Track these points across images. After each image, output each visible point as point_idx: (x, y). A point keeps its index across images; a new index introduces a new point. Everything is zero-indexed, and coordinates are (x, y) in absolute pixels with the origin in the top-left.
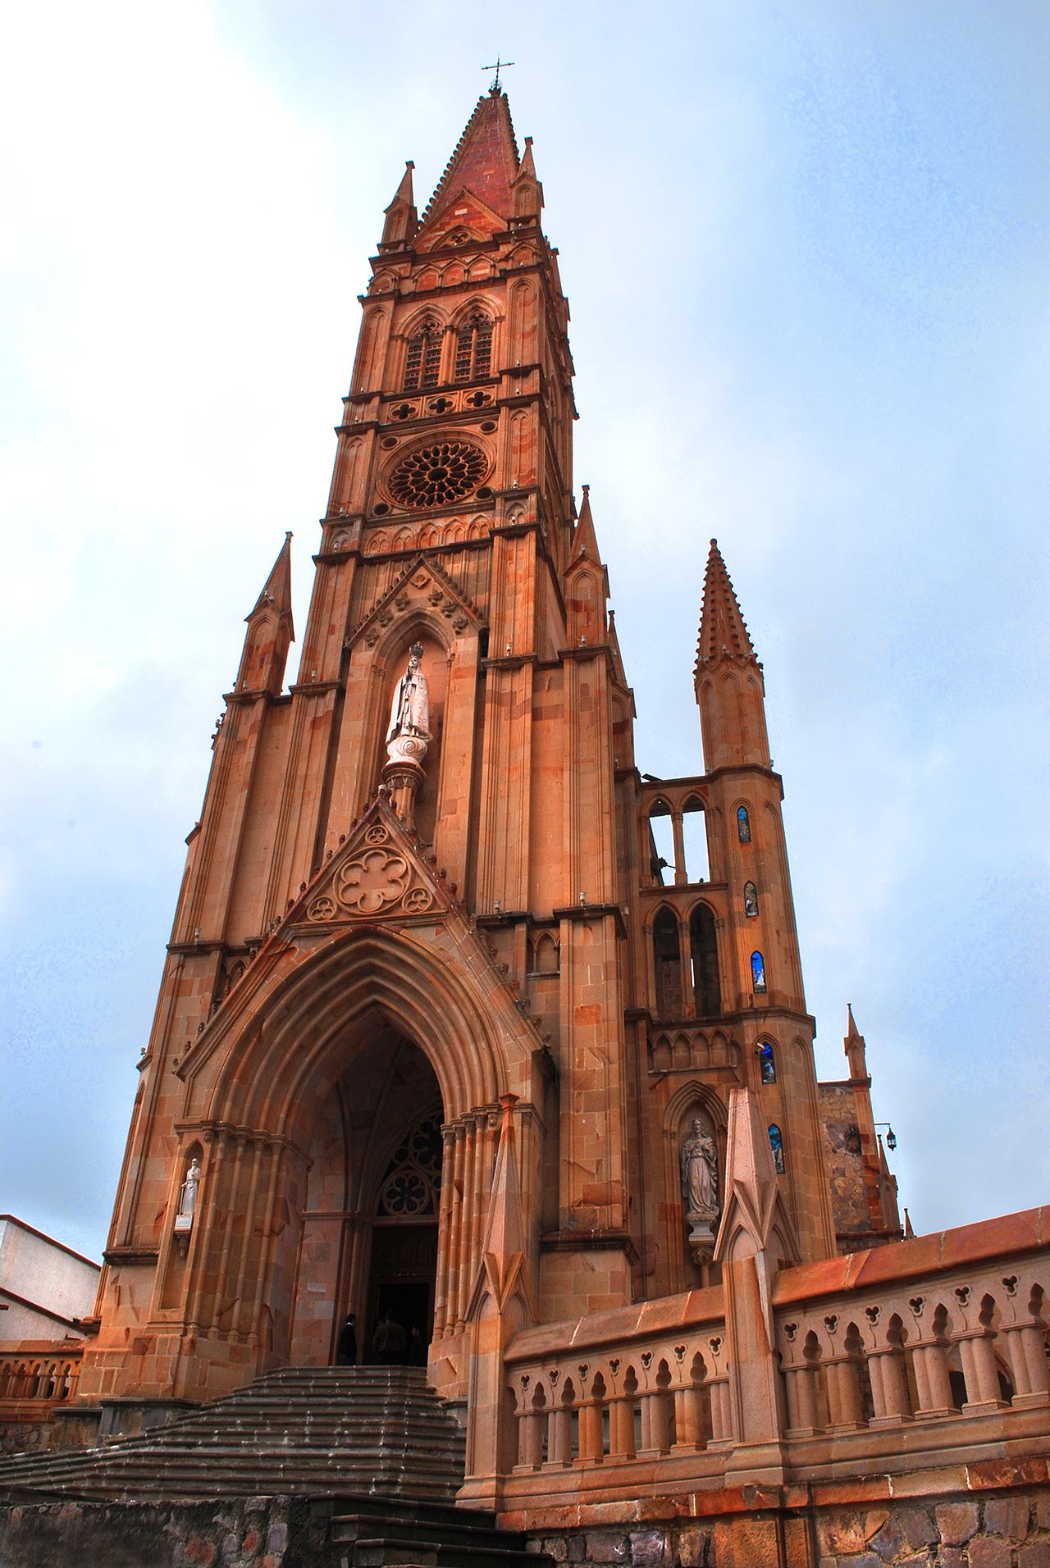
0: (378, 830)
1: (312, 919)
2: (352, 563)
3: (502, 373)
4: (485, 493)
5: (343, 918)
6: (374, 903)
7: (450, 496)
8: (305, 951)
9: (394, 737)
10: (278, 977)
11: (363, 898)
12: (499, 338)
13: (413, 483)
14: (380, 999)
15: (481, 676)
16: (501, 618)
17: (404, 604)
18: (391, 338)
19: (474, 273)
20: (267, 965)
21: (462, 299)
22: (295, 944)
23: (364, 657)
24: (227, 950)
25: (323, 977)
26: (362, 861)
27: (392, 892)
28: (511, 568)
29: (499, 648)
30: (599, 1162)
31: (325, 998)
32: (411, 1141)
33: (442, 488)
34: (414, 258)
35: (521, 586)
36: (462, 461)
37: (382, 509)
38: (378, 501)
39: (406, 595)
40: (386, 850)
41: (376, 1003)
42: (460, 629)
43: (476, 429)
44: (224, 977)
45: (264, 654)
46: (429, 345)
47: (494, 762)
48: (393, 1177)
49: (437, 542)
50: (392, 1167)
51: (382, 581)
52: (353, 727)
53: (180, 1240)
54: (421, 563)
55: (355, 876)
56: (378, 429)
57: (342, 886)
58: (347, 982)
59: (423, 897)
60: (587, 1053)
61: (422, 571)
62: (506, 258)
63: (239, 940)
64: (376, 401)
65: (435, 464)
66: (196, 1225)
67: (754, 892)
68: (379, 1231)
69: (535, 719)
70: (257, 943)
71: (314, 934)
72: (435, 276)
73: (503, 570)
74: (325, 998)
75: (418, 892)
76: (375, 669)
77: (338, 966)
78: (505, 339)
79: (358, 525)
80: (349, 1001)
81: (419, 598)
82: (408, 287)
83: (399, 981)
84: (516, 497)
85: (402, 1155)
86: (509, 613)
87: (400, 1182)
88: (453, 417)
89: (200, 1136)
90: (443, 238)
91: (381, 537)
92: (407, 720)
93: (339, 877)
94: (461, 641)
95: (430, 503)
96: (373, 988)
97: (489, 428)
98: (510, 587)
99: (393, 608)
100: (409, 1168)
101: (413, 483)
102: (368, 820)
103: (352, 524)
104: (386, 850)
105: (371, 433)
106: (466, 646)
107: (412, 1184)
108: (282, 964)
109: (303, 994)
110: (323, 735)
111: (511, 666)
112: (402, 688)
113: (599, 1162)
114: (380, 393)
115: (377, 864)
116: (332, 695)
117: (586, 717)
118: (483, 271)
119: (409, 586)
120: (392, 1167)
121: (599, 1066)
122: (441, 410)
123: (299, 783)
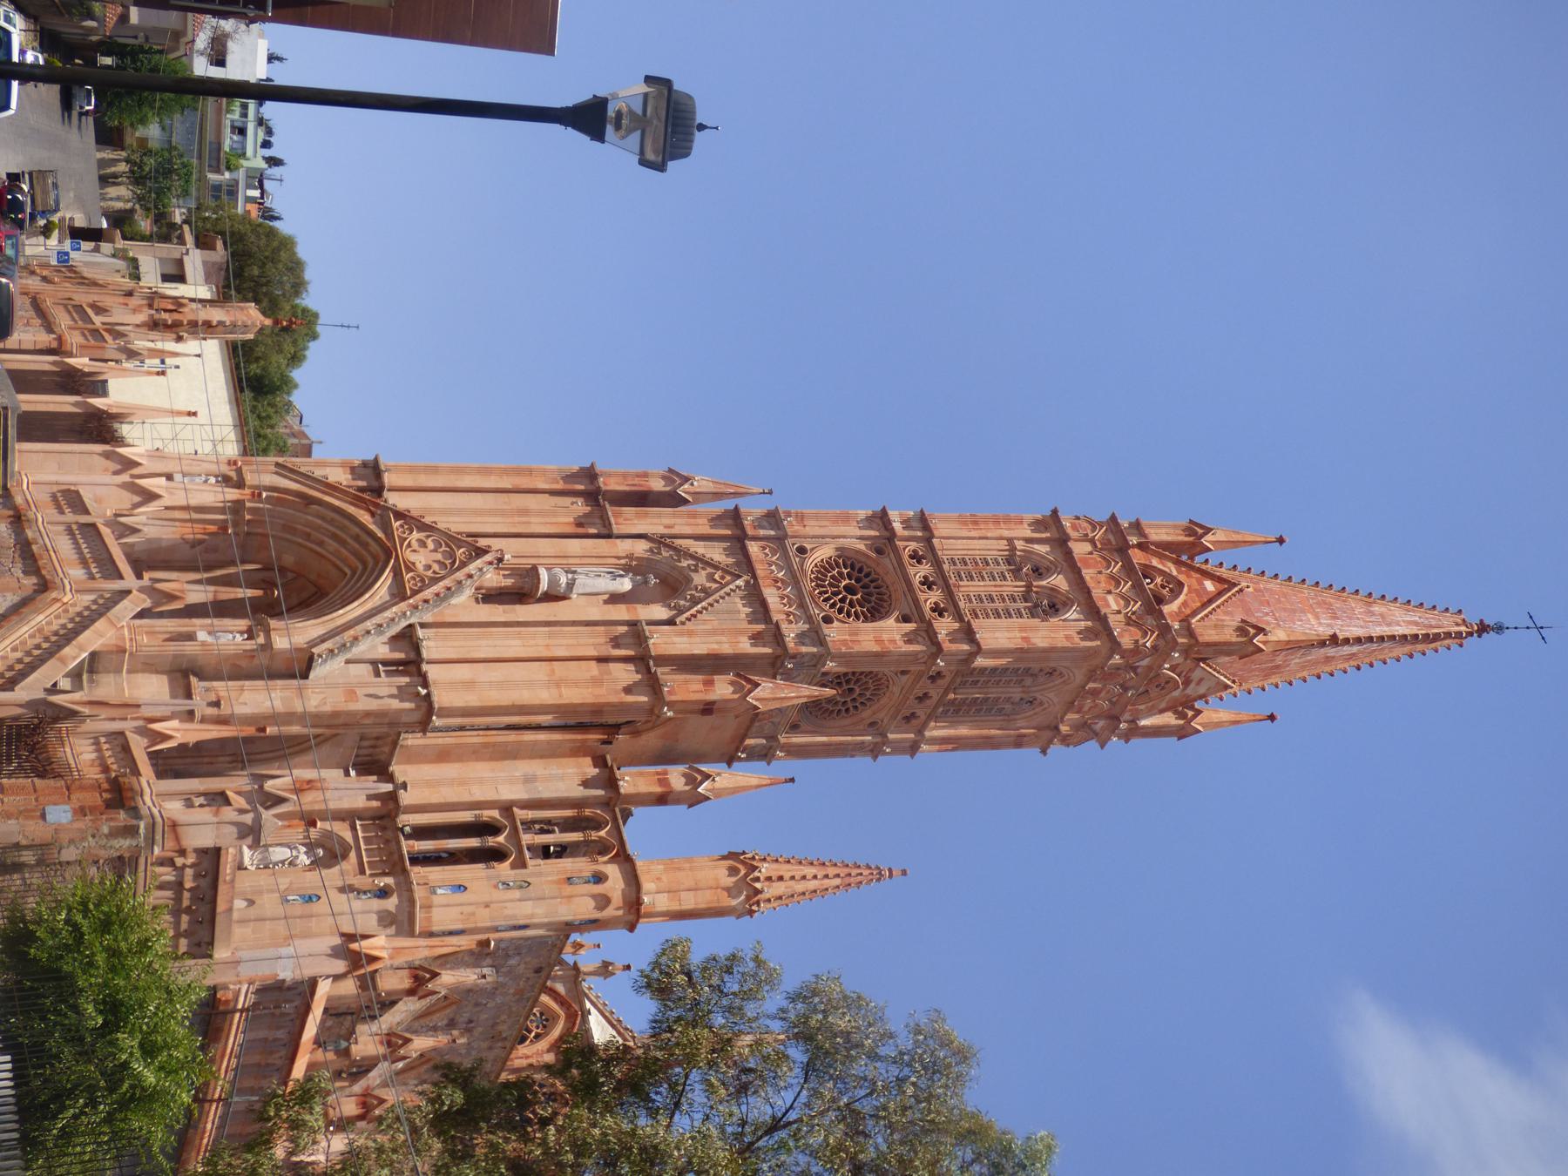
1: (396, 524)
6: (412, 557)
10: (351, 510)
16: (690, 634)
19: (1110, 598)
23: (641, 548)
25: (357, 538)
27: (420, 567)
31: (342, 542)
33: (835, 594)
55: (431, 545)
58: (355, 554)
74: (342, 542)
76: (630, 557)
77: (365, 545)
80: (344, 560)
81: (700, 578)
82: (1080, 549)
84: (814, 635)
114: (932, 536)
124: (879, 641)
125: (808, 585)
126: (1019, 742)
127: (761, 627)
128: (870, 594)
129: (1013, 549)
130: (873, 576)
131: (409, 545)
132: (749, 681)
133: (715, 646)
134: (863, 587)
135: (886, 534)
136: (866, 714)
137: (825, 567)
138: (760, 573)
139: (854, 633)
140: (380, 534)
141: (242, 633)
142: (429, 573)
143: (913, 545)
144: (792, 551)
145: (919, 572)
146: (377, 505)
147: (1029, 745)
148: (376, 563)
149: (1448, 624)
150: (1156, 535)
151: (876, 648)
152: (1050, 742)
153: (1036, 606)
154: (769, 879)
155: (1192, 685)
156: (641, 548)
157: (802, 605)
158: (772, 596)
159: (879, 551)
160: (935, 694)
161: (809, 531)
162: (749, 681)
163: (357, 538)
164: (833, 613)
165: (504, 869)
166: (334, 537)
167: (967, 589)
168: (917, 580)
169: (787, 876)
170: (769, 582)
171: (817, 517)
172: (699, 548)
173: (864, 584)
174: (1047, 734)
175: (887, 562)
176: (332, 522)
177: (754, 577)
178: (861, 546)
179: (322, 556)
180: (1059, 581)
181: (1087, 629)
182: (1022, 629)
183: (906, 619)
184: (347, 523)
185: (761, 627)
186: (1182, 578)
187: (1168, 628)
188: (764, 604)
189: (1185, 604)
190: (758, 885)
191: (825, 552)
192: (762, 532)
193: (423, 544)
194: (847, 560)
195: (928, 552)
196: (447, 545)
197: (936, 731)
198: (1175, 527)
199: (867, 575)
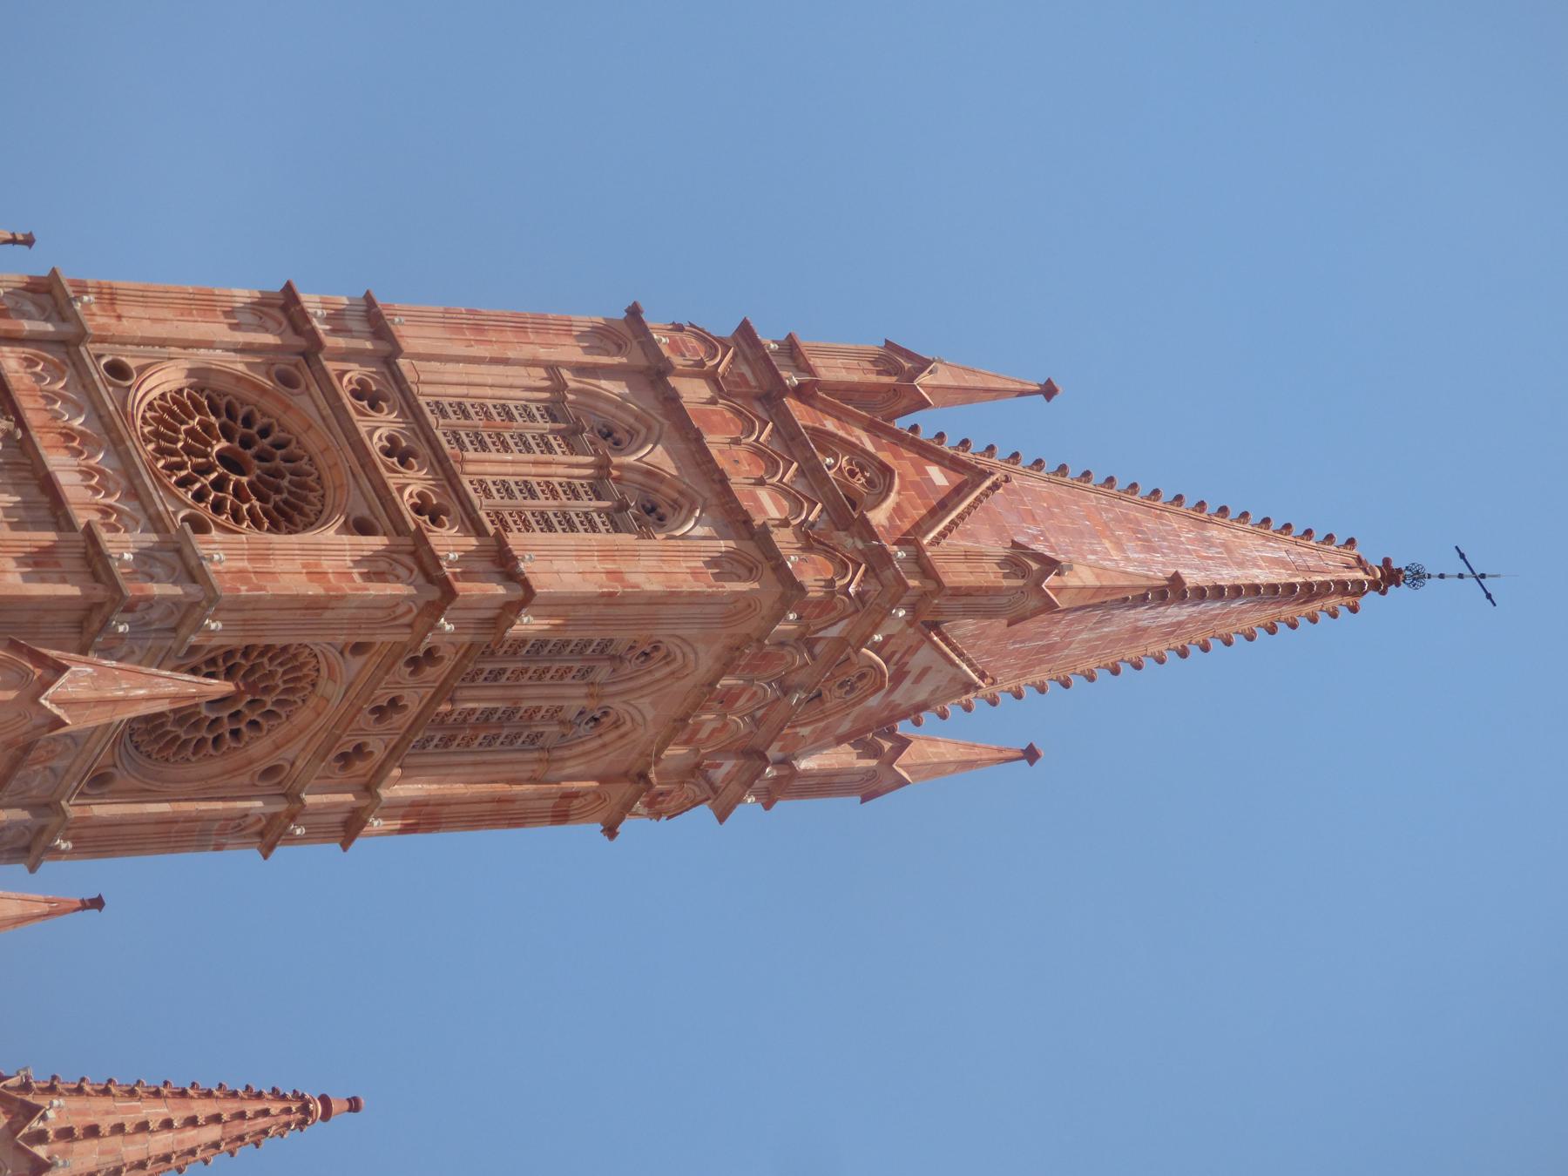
7: (183, 483)
19: (763, 495)
33: (203, 470)
82: (693, 392)
114: (397, 351)
124: (316, 575)
126: (561, 815)
127: (48, 537)
128: (278, 474)
129: (559, 387)
130: (277, 434)
132: (40, 660)
134: (260, 457)
135: (300, 342)
136: (259, 748)
137: (170, 411)
138: (33, 418)
139: (262, 556)
143: (355, 371)
144: (98, 374)
145: (377, 428)
147: (584, 816)
149: (1332, 566)
150: (831, 370)
151: (314, 590)
152: (626, 809)
153: (622, 507)
154: (66, 1134)
155: (907, 683)
157: (134, 492)
158: (63, 468)
159: (287, 380)
160: (413, 701)
161: (128, 327)
162: (40, 660)
164: (204, 510)
167: (483, 467)
168: (375, 444)
169: (105, 1125)
170: (51, 438)
171: (144, 298)
173: (251, 452)
174: (625, 789)
175: (307, 403)
177: (20, 423)
178: (238, 365)
180: (657, 456)
181: (729, 556)
182: (607, 554)
183: (362, 527)
185: (48, 537)
186: (885, 457)
187: (887, 558)
188: (48, 485)
189: (898, 510)
190: (41, 1151)
191: (167, 379)
192: (27, 326)
195: (389, 385)
197: (401, 790)
198: (859, 355)
199: (264, 432)
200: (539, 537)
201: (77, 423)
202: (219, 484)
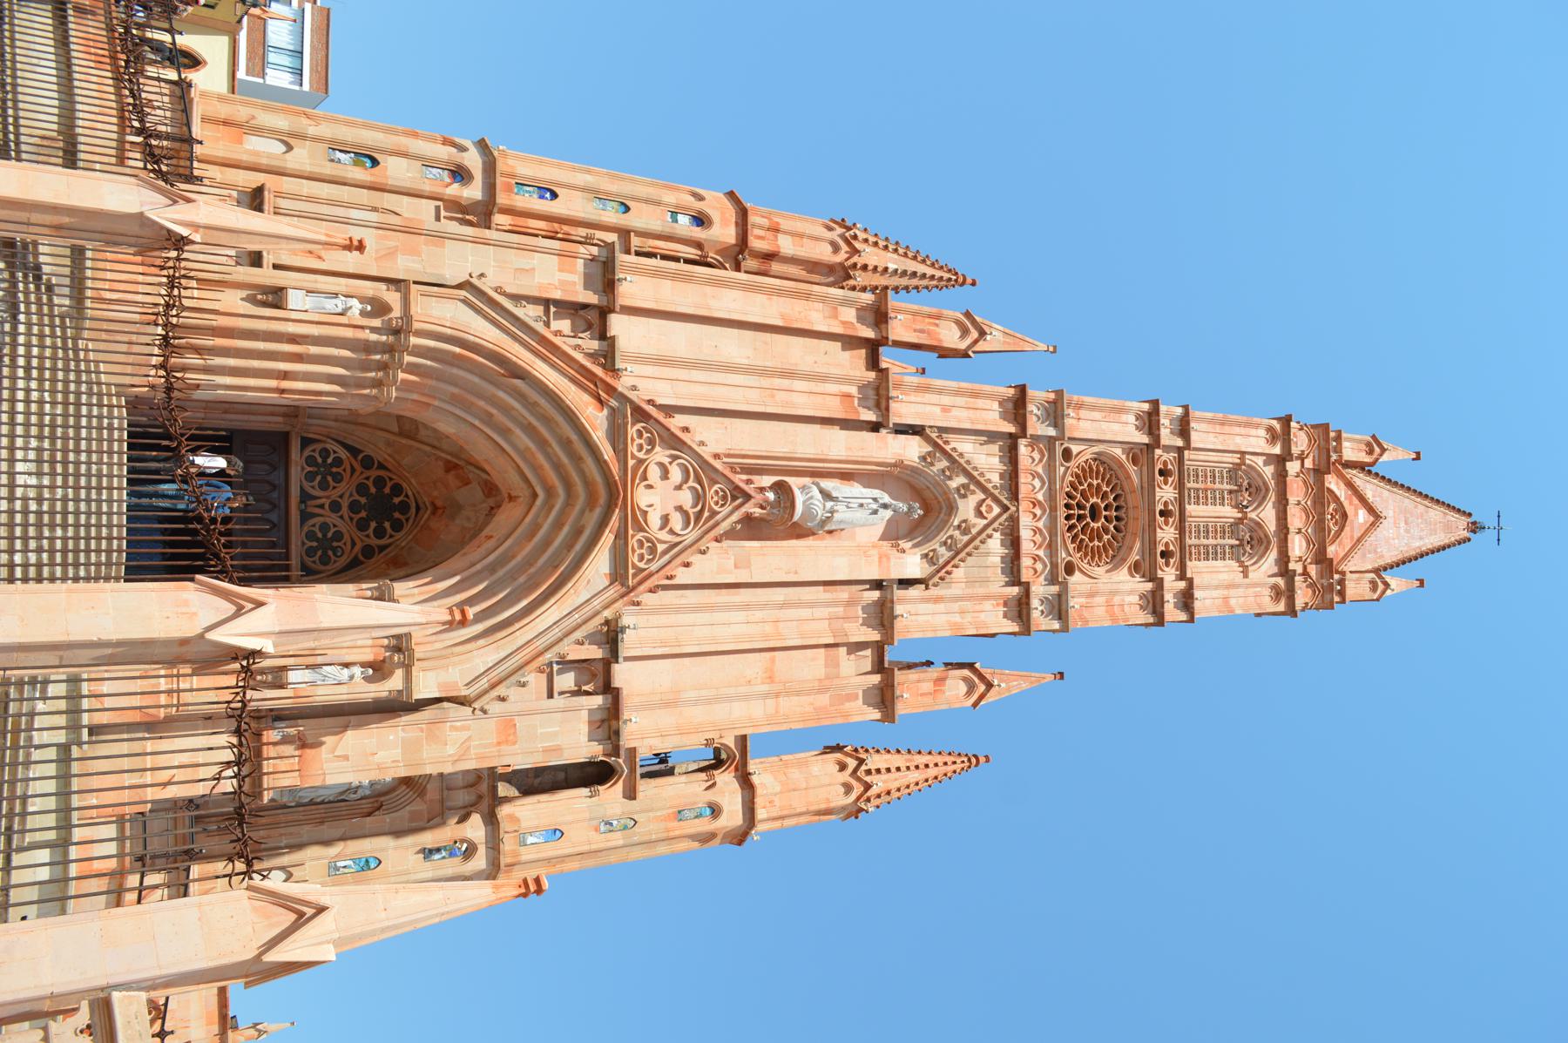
0: (724, 498)
1: (632, 431)
2: (1011, 429)
3: (1190, 582)
4: (1070, 569)
5: (631, 463)
6: (642, 497)
8: (595, 419)
9: (822, 491)
11: (650, 487)
12: (1226, 570)
13: (1090, 485)
14: (539, 502)
15: (878, 585)
16: (938, 600)
17: (963, 492)
18: (1243, 453)
19: (1297, 538)
20: (584, 378)
21: (1271, 525)
22: (605, 411)
23: (911, 450)
24: (604, 312)
25: (566, 444)
26: (691, 483)
27: (654, 520)
28: (988, 605)
29: (903, 601)
30: (346, 758)
31: (542, 444)
32: (382, 473)
33: (1080, 518)
34: (1320, 472)
35: (969, 618)
36: (1106, 537)
37: (1067, 455)
38: (1075, 449)
39: (973, 492)
40: (701, 511)
41: (535, 495)
42: (929, 558)
43: (1135, 556)
44: (573, 309)
45: (929, 333)
46: (1230, 492)
47: (784, 605)
48: (343, 454)
49: (1025, 521)
50: (354, 451)
51: (988, 461)
52: (840, 445)
53: (274, 297)
54: (1005, 509)
55: (676, 474)
56: (1150, 448)
57: (666, 460)
58: (558, 467)
59: (647, 557)
60: (464, 735)
61: (997, 510)
62: (1305, 573)
63: (618, 325)
64: (1180, 443)
65: (1106, 508)
66: (294, 315)
67: (625, 827)
68: (285, 437)
69: (827, 646)
70: (608, 355)
71: (617, 435)
72: (1297, 493)
73: (987, 597)
74: (542, 444)
75: (653, 550)
77: (576, 459)
78: (1224, 577)
79: (1052, 432)
80: (536, 469)
81: (966, 509)
82: (1293, 467)
83: (558, 525)
85: (368, 463)
86: (941, 607)
87: (338, 462)
88: (1152, 527)
89: (397, 312)
90: (1336, 499)
91: (1036, 455)
92: (840, 507)
93: (675, 458)
94: (917, 558)
95: (1067, 506)
96: (550, 492)
97: (1136, 567)
98: (967, 605)
99: (962, 480)
100: (353, 470)
101: (1090, 485)
102: (737, 488)
103: (1055, 426)
104: (701, 511)
105: (1145, 439)
106: (912, 564)
107: (334, 549)
108: (586, 398)
109: (547, 420)
110: (835, 409)
111: (883, 616)
112: (875, 500)
113: (346, 758)
114: (1188, 446)
115: (686, 498)
116: (870, 416)
117: (824, 700)
118: (1297, 547)
119: (983, 496)
120: (354, 451)
121: (451, 750)
122: (1162, 513)
123: (785, 383)
125: (1062, 512)
131: (645, 478)
133: (957, 618)
140: (607, 453)
141: (364, 665)
142: (664, 535)
146: (611, 390)
148: (591, 502)
150: (1351, 452)
153: (1241, 545)
156: (911, 450)
157: (1051, 548)
163: (566, 444)
164: (1076, 558)
165: (612, 794)
166: (530, 430)
171: (1093, 408)
172: (965, 447)
176: (531, 406)
178: (1118, 452)
179: (503, 450)
184: (560, 419)
186: (1346, 504)
187: (1331, 587)
193: (665, 475)
194: (1103, 466)
196: (699, 480)
198: (1360, 441)
200: (1203, 564)
201: (1040, 497)
202: (1080, 518)
